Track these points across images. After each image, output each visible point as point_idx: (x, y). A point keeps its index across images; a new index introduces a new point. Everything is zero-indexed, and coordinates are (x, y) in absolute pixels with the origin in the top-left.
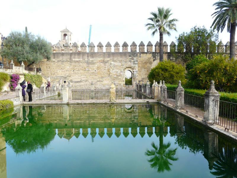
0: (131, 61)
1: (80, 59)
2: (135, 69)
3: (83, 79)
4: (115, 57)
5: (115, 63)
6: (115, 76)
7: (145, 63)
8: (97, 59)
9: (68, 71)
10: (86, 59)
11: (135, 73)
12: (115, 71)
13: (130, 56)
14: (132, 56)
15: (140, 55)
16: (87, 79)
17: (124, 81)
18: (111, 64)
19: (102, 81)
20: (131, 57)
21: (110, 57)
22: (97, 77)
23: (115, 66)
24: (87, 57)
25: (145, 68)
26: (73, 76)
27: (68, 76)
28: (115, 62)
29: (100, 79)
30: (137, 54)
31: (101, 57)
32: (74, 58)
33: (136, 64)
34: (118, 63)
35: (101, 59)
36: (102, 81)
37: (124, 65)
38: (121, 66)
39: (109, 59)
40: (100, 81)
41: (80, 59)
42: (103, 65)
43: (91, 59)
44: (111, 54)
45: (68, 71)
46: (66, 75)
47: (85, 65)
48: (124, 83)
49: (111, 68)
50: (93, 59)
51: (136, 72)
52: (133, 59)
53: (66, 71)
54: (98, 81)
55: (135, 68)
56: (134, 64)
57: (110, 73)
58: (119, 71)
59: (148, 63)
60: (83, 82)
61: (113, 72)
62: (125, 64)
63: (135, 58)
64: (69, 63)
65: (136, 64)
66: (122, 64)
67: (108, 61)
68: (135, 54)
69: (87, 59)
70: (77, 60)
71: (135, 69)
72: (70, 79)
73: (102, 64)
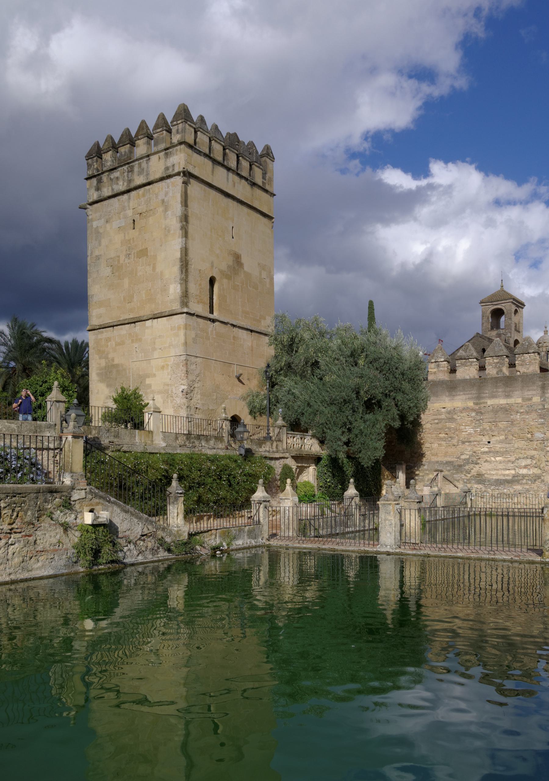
1: (511, 401)
3: (524, 471)
9: (470, 442)
10: (536, 399)
16: (537, 471)
32: (493, 397)
41: (511, 401)
45: (470, 442)
46: (463, 457)
47: (532, 420)
53: (463, 443)
60: (524, 481)
64: (473, 414)
69: (541, 398)
70: (502, 401)
72: (474, 472)
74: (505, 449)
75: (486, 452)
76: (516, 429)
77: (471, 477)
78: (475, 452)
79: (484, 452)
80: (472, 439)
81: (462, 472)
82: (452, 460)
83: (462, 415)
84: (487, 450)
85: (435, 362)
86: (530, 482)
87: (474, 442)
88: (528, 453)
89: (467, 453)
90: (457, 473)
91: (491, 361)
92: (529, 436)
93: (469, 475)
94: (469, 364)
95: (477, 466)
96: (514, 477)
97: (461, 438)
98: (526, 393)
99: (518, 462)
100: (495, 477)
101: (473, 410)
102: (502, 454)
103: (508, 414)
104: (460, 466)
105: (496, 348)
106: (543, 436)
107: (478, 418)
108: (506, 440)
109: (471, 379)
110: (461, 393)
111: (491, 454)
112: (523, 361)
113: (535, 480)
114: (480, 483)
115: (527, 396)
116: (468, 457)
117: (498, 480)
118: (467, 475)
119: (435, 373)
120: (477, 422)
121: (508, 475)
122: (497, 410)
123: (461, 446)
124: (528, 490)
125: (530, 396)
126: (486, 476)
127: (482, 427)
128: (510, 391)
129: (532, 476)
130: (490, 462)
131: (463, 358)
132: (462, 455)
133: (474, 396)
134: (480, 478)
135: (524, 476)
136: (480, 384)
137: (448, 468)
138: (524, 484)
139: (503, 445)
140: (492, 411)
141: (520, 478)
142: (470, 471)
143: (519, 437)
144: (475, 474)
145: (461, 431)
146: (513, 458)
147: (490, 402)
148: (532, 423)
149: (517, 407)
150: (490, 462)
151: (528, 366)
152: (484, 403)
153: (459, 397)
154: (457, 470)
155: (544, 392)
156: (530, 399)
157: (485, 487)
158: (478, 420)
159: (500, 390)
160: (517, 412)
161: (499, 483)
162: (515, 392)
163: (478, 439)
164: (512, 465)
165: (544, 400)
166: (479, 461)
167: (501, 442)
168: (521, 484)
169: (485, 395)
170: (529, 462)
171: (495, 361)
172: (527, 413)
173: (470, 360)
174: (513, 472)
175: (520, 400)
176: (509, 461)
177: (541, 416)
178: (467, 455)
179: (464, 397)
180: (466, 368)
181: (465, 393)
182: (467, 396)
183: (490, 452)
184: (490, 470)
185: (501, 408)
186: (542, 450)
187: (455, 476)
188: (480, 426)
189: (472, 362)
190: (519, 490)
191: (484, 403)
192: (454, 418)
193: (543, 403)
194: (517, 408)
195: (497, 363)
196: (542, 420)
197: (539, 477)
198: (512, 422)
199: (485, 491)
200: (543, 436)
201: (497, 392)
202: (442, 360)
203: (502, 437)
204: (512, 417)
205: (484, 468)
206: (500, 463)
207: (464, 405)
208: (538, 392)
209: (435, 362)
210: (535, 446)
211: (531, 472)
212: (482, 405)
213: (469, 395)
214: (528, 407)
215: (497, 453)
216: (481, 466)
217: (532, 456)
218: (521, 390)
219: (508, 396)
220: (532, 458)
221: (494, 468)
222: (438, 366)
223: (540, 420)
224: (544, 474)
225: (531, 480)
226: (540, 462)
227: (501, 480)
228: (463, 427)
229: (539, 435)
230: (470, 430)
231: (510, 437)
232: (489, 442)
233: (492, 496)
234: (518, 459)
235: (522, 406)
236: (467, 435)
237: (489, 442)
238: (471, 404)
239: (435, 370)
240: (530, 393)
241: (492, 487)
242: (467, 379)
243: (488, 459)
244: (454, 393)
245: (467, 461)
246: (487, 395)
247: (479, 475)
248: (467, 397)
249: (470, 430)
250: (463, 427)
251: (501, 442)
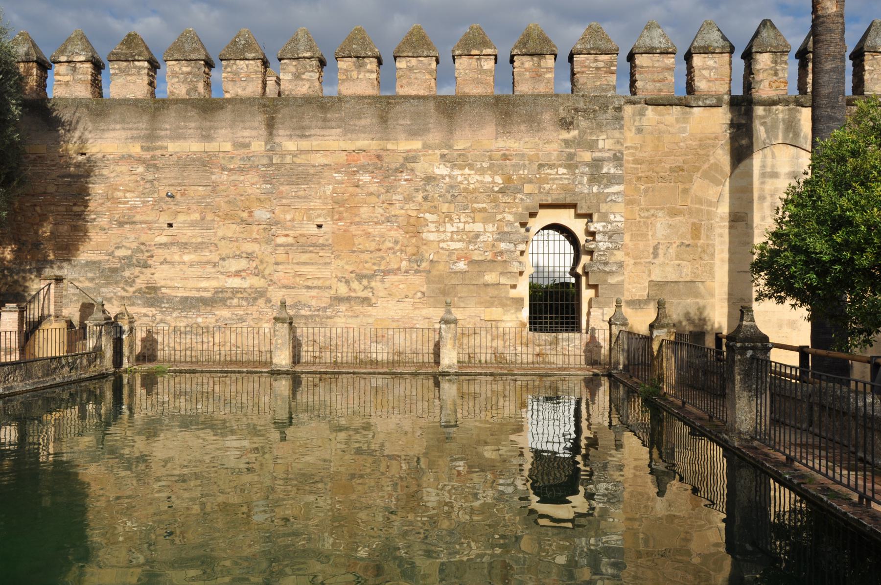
0: (571, 156)
2: (604, 218)
3: (235, 283)
4: (458, 134)
5: (456, 172)
6: (462, 265)
7: (672, 170)
8: (328, 146)
9: (134, 223)
10: (258, 146)
11: (602, 246)
12: (461, 225)
13: (566, 124)
14: (583, 123)
15: (642, 114)
17: (520, 301)
18: (430, 179)
19: (366, 301)
20: (575, 133)
21: (425, 130)
22: (326, 273)
23: (459, 196)
24: (263, 131)
25: (673, 213)
26: (165, 262)
27: (130, 258)
28: (461, 168)
29: (355, 285)
30: (619, 109)
31: (363, 130)
33: (612, 180)
34: (482, 171)
35: (362, 143)
36: (366, 301)
37: (527, 188)
38: (502, 191)
39: (417, 145)
40: (348, 299)
42: (373, 188)
43: (290, 145)
44: (431, 105)
46: (120, 253)
47: (252, 185)
48: (525, 314)
49: (434, 210)
50: (305, 144)
51: (610, 235)
52: (591, 146)
53: (121, 224)
54: (339, 300)
55: (604, 208)
56: (594, 179)
57: (426, 243)
58: (490, 228)
59: (696, 176)
60: (235, 301)
61: (443, 237)
62: (530, 182)
63: (605, 143)
64: (141, 169)
65: (610, 183)
66: (508, 179)
67: (411, 158)
68: (604, 107)
70: (195, 146)
71: (604, 218)
72: (140, 283)
73: (366, 178)
74: (200, 240)
75: (165, 244)
76: (220, 201)
77: (134, 292)
78: (143, 244)
79: (161, 244)
80: (138, 218)
81: (117, 283)
82: (99, 258)
83: (118, 169)
84: (163, 239)
85: (69, 62)
86: (245, 303)
87: (141, 223)
88: (243, 249)
89: (128, 245)
90: (108, 284)
91: (176, 69)
92: (245, 215)
93: (131, 290)
94: (134, 71)
95: (148, 271)
96: (216, 292)
97: (117, 216)
98: (240, 134)
99: (224, 263)
100: (181, 294)
101: (140, 160)
102: (198, 247)
103: (205, 171)
104: (114, 271)
105: (186, 45)
106: (268, 215)
107: (150, 177)
108: (201, 223)
109: (137, 100)
110: (118, 126)
111: (175, 249)
112: (236, 73)
113: (255, 299)
114: (149, 306)
115: (241, 140)
116: (129, 253)
117: (187, 298)
118: (128, 288)
119: (67, 84)
120: (148, 185)
121: (205, 289)
122: (185, 163)
123: (115, 231)
124: (242, 319)
125: (247, 140)
126: (164, 290)
127: (156, 195)
128: (210, 128)
129: (249, 291)
130: (171, 263)
131: (122, 57)
132: (117, 248)
133: (143, 133)
134: (152, 295)
135: (235, 291)
136: (154, 106)
137: (90, 275)
138: (234, 307)
139: (197, 231)
140: (177, 164)
141: (229, 295)
142: (134, 281)
143: (227, 217)
144: (143, 286)
145: (117, 201)
146: (215, 257)
147: (172, 147)
148: (250, 192)
149: (224, 158)
150: (171, 263)
151: (244, 84)
152: (161, 148)
153: (112, 134)
154: (107, 278)
155: (271, 134)
156: (247, 146)
157: (162, 312)
158: (151, 182)
159: (193, 125)
160: (223, 169)
161: (188, 304)
162: (219, 131)
163: (149, 219)
164: (213, 270)
165: (272, 149)
166: (150, 262)
167: (193, 224)
168: (229, 307)
169: (163, 133)
170: (243, 264)
171: (185, 69)
172: (242, 170)
173: (136, 63)
174: (214, 284)
175: (228, 147)
176: (208, 262)
177: (266, 179)
178: (129, 248)
179: (123, 134)
180: (129, 78)
181: (126, 126)
182: (129, 134)
183: (172, 244)
184: (171, 279)
185: (194, 160)
186: (268, 242)
187: (103, 290)
188: (154, 192)
189: (140, 68)
190: (225, 319)
191: (161, 148)
192: (103, 175)
193: (270, 153)
194: (222, 162)
195: (189, 73)
196: (269, 186)
197: (259, 294)
198: (214, 188)
199: (162, 321)
200: (268, 215)
201: (186, 127)
202: (82, 58)
203: (196, 216)
204: (213, 177)
205: (161, 275)
206: (191, 265)
207: (124, 151)
208: (261, 132)
209: (69, 62)
210: (255, 235)
211: (245, 284)
212: (158, 153)
213: (134, 132)
214: (242, 159)
215: (184, 246)
216: (153, 271)
217: (249, 254)
218: (232, 128)
219: (207, 137)
220: (250, 256)
221: (176, 275)
222: (74, 69)
223: (264, 186)
224: (270, 288)
225: (247, 299)
226: (265, 265)
227: (192, 298)
228: (119, 194)
229: (262, 214)
230: (133, 199)
231: (209, 217)
232: (170, 225)
233: (175, 330)
234: (223, 259)
235: (233, 158)
236: (129, 209)
237: (170, 225)
238: (136, 149)
239: (67, 78)
240: (247, 133)
241: (175, 314)
242: (129, 100)
243: (169, 258)
244: (102, 126)
245: (128, 262)
246: (168, 132)
247: (153, 289)
248: (130, 136)
249: (133, 199)
250: (119, 194)
251: (193, 224)
